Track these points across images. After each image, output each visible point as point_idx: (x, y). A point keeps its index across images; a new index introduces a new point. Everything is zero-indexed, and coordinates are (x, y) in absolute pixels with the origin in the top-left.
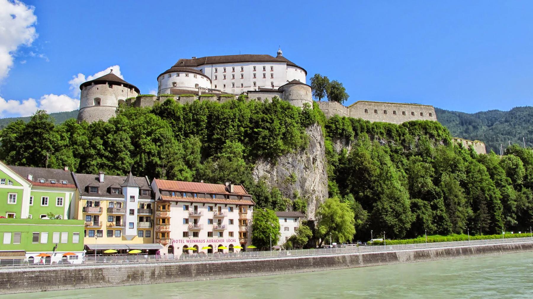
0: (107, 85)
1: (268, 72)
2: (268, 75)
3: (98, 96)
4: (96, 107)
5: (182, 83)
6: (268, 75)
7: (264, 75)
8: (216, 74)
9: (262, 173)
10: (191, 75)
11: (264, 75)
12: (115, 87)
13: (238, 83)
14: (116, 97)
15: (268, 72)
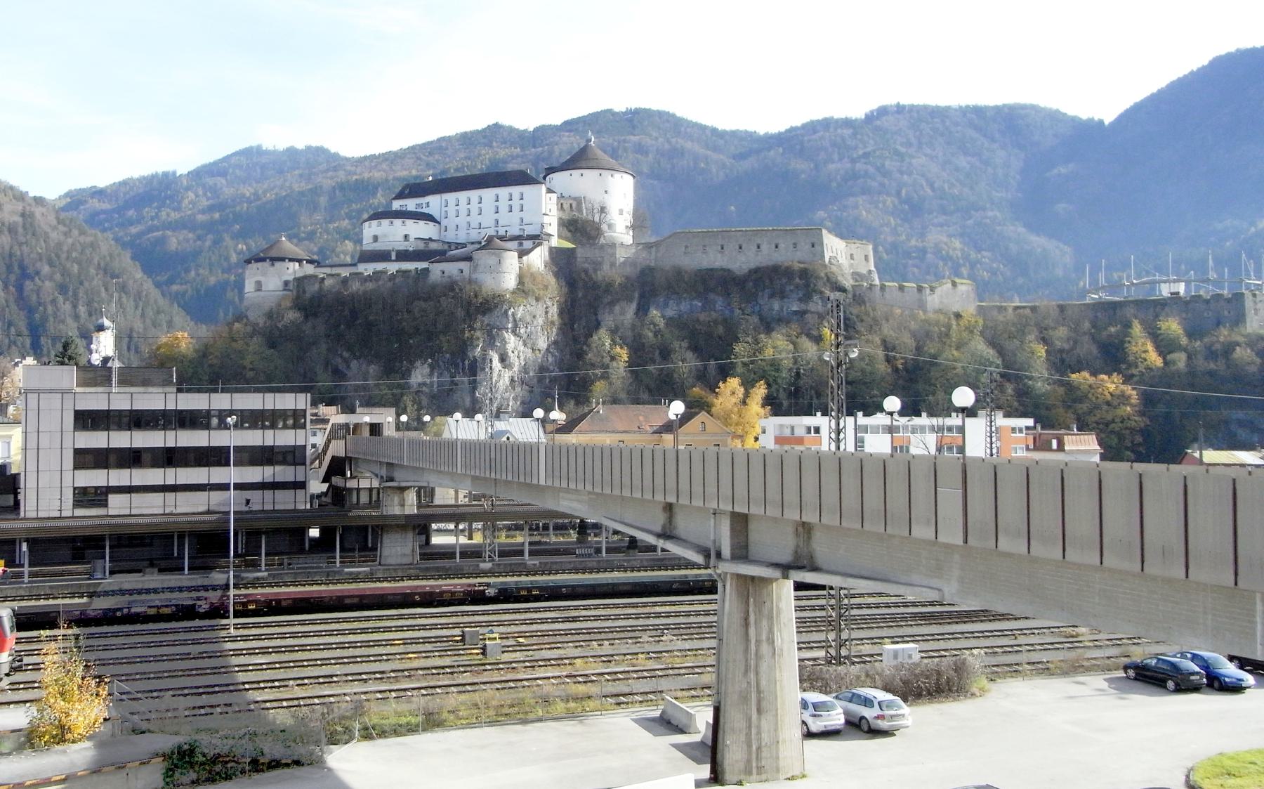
0: (267, 264)
1: (516, 203)
2: (516, 208)
3: (259, 278)
4: (259, 293)
5: (385, 236)
6: (516, 208)
7: (511, 207)
8: (446, 209)
9: (420, 380)
10: (398, 222)
11: (511, 207)
12: (278, 264)
13: (474, 224)
14: (280, 277)
15: (516, 203)
